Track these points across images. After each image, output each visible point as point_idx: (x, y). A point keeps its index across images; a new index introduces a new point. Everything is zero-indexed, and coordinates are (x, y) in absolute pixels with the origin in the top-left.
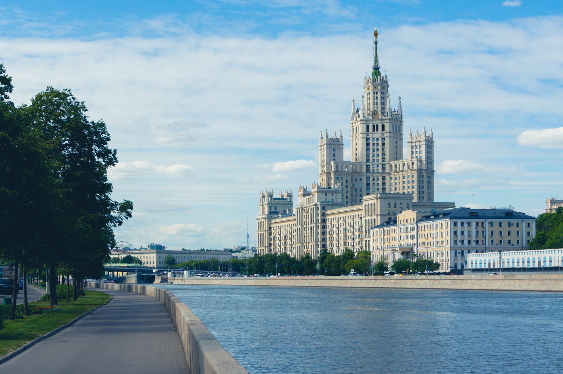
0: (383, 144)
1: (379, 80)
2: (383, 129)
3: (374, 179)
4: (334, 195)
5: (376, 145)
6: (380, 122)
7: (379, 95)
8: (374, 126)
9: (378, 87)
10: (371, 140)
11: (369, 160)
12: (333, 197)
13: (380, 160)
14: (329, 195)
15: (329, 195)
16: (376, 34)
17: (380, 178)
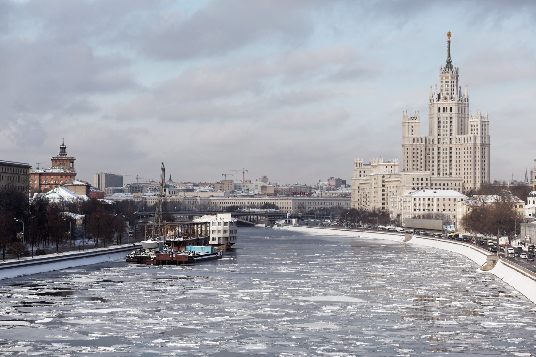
0: (451, 122)
1: (450, 72)
2: (451, 111)
3: (443, 150)
4: (393, 167)
5: (445, 123)
6: (449, 105)
7: (450, 84)
8: (444, 108)
9: (449, 78)
10: (442, 118)
11: (440, 134)
12: (392, 169)
13: (449, 135)
14: (389, 167)
15: (389, 167)
16: (449, 35)
17: (448, 149)
